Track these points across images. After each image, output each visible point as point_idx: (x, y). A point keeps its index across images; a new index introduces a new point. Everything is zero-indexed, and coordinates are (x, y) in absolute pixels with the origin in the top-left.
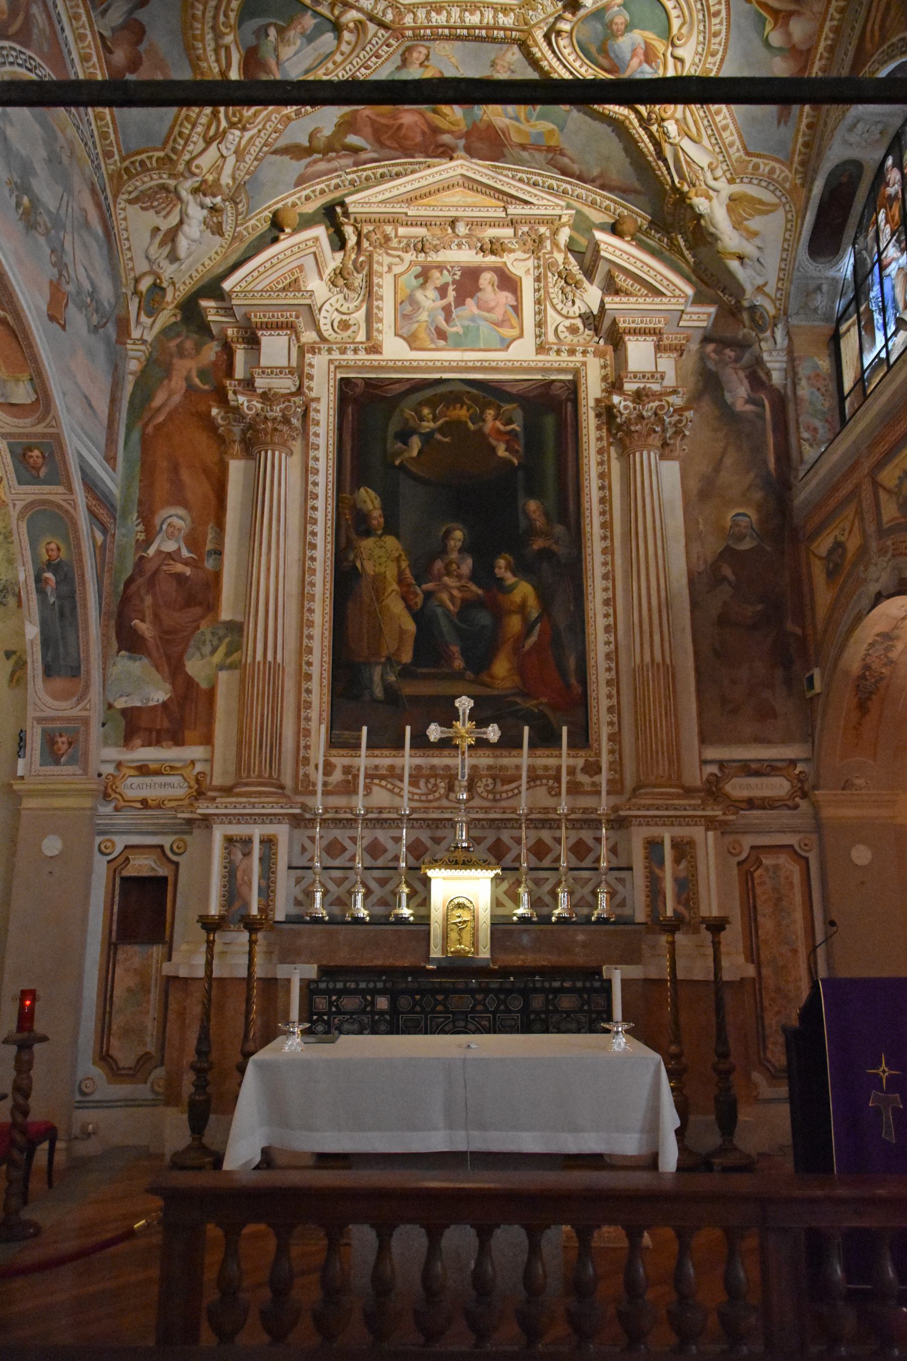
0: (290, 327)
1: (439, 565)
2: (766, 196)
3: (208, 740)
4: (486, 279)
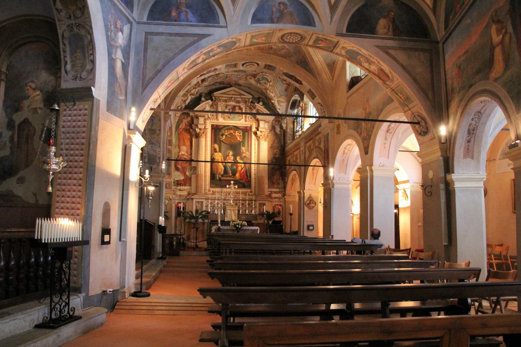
0: (204, 116)
1: (228, 158)
2: (283, 100)
3: (190, 185)
4: (237, 108)
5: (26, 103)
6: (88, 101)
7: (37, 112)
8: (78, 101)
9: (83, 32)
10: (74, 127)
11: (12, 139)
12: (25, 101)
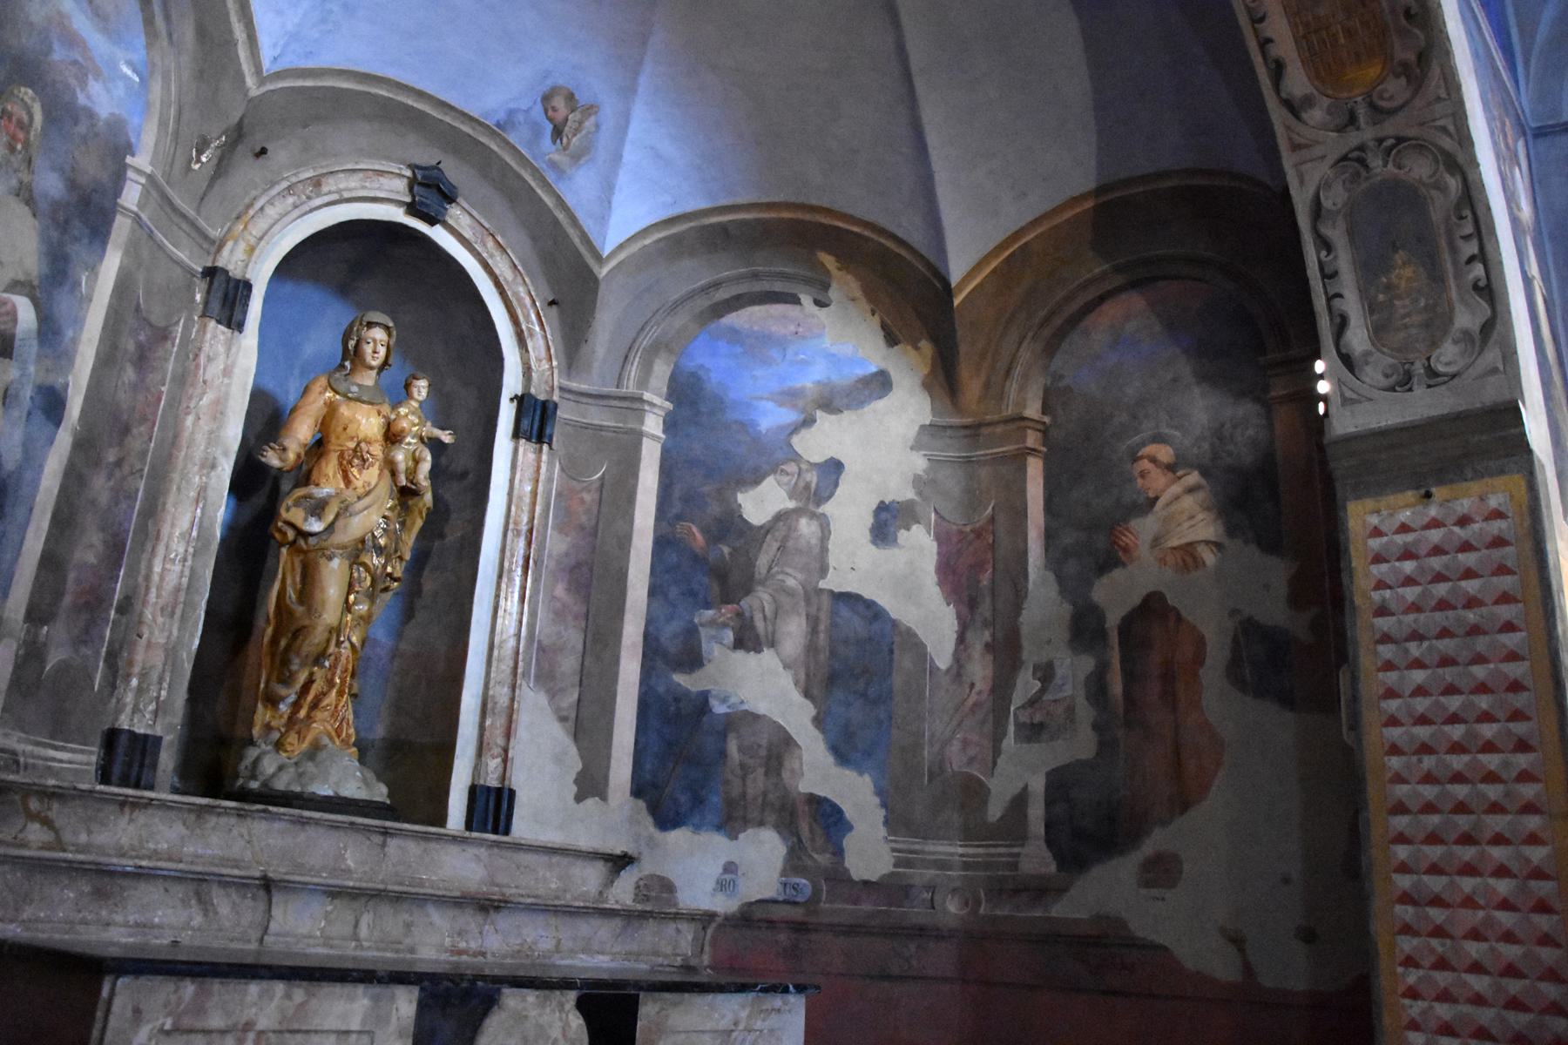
5: (1143, 529)
6: (1502, 472)
7: (1198, 563)
8: (1441, 483)
9: (1419, 169)
10: (1443, 605)
11: (1097, 687)
12: (1135, 524)
